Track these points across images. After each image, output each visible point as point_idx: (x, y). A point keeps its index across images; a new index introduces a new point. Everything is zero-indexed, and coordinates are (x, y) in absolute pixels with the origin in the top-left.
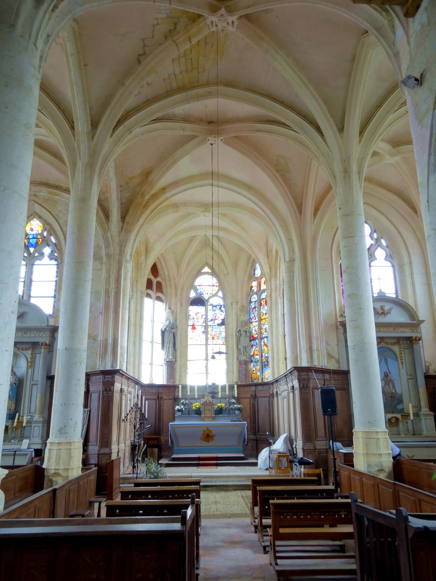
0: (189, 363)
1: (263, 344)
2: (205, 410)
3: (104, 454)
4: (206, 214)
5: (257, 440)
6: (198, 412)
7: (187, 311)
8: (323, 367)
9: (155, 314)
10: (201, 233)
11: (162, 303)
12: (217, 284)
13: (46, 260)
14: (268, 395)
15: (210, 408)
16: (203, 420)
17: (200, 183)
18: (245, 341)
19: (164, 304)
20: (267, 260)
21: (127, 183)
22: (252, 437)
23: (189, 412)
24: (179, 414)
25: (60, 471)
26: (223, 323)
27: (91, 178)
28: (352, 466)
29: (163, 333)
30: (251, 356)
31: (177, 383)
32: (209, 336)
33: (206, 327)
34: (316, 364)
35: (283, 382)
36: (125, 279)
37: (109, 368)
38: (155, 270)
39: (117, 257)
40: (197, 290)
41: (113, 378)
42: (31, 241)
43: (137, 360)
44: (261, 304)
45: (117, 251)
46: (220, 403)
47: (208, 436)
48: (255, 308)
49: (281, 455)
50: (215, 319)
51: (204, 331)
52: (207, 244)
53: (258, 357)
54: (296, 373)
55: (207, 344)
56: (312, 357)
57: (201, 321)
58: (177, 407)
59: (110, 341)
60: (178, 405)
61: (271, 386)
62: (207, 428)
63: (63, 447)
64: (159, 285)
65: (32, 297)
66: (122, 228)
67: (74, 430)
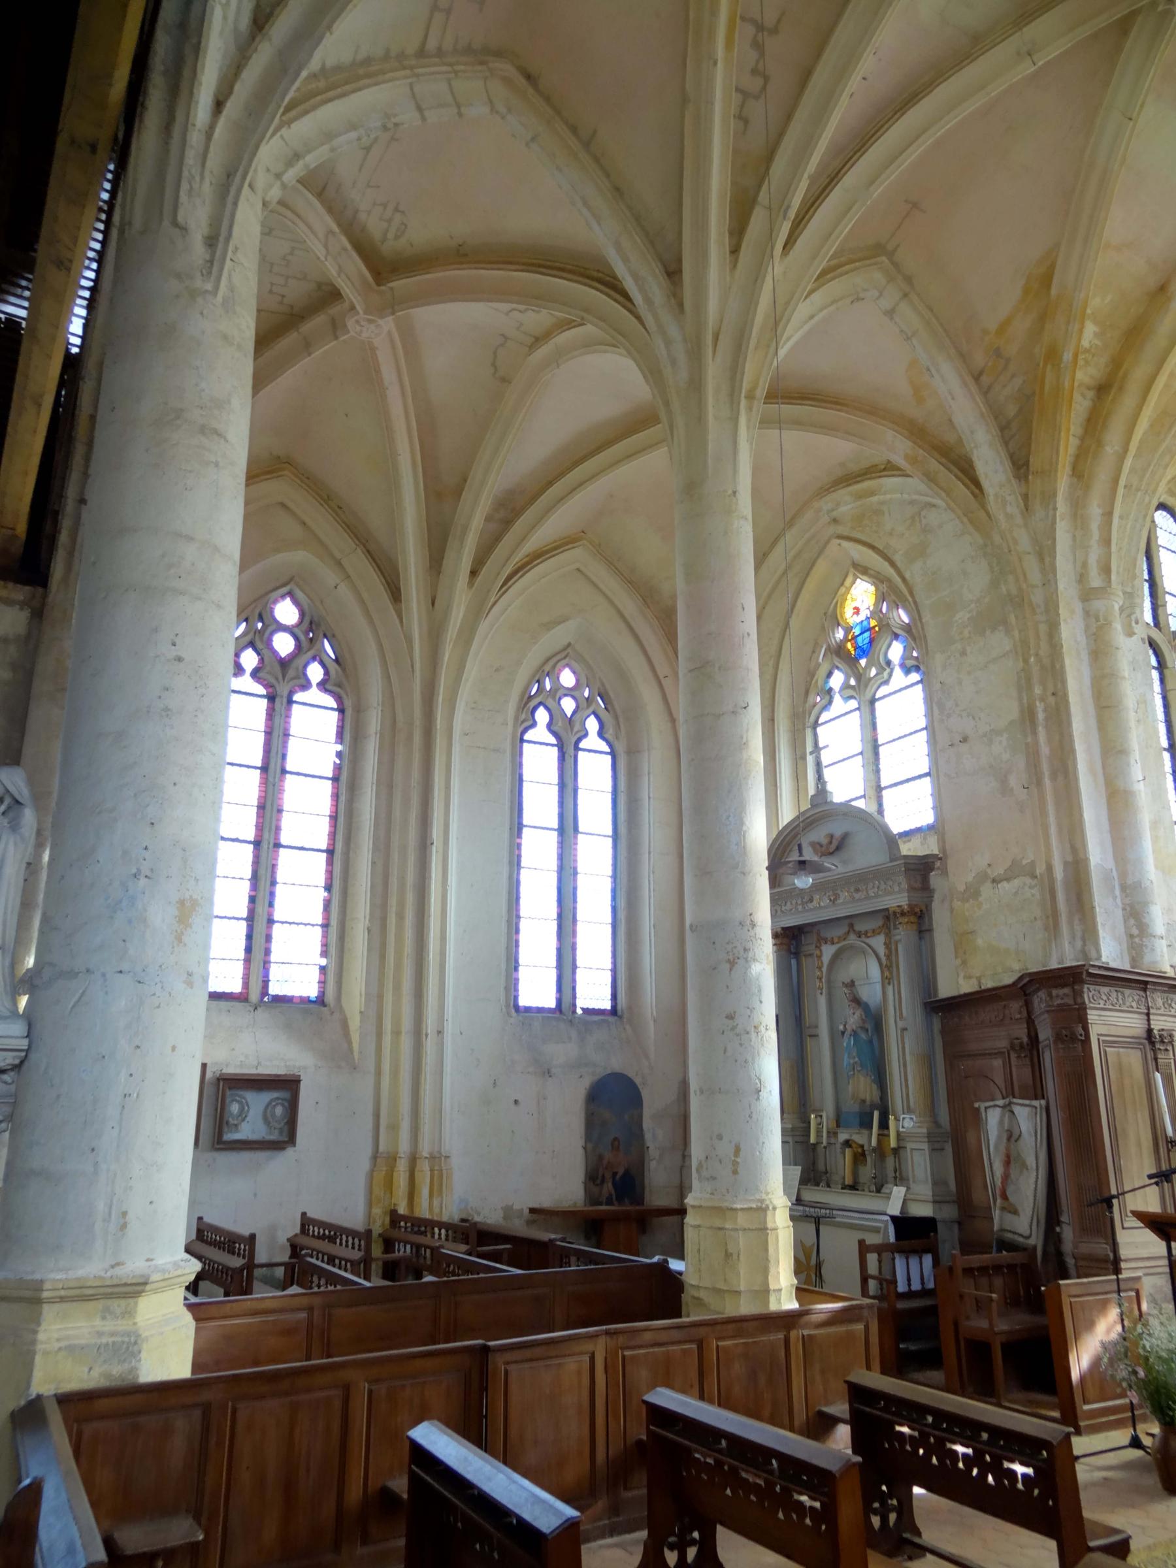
13: (899, 678)
21: (998, 353)
45: (1035, 576)
65: (886, 788)
66: (1025, 497)
67: (735, 1172)
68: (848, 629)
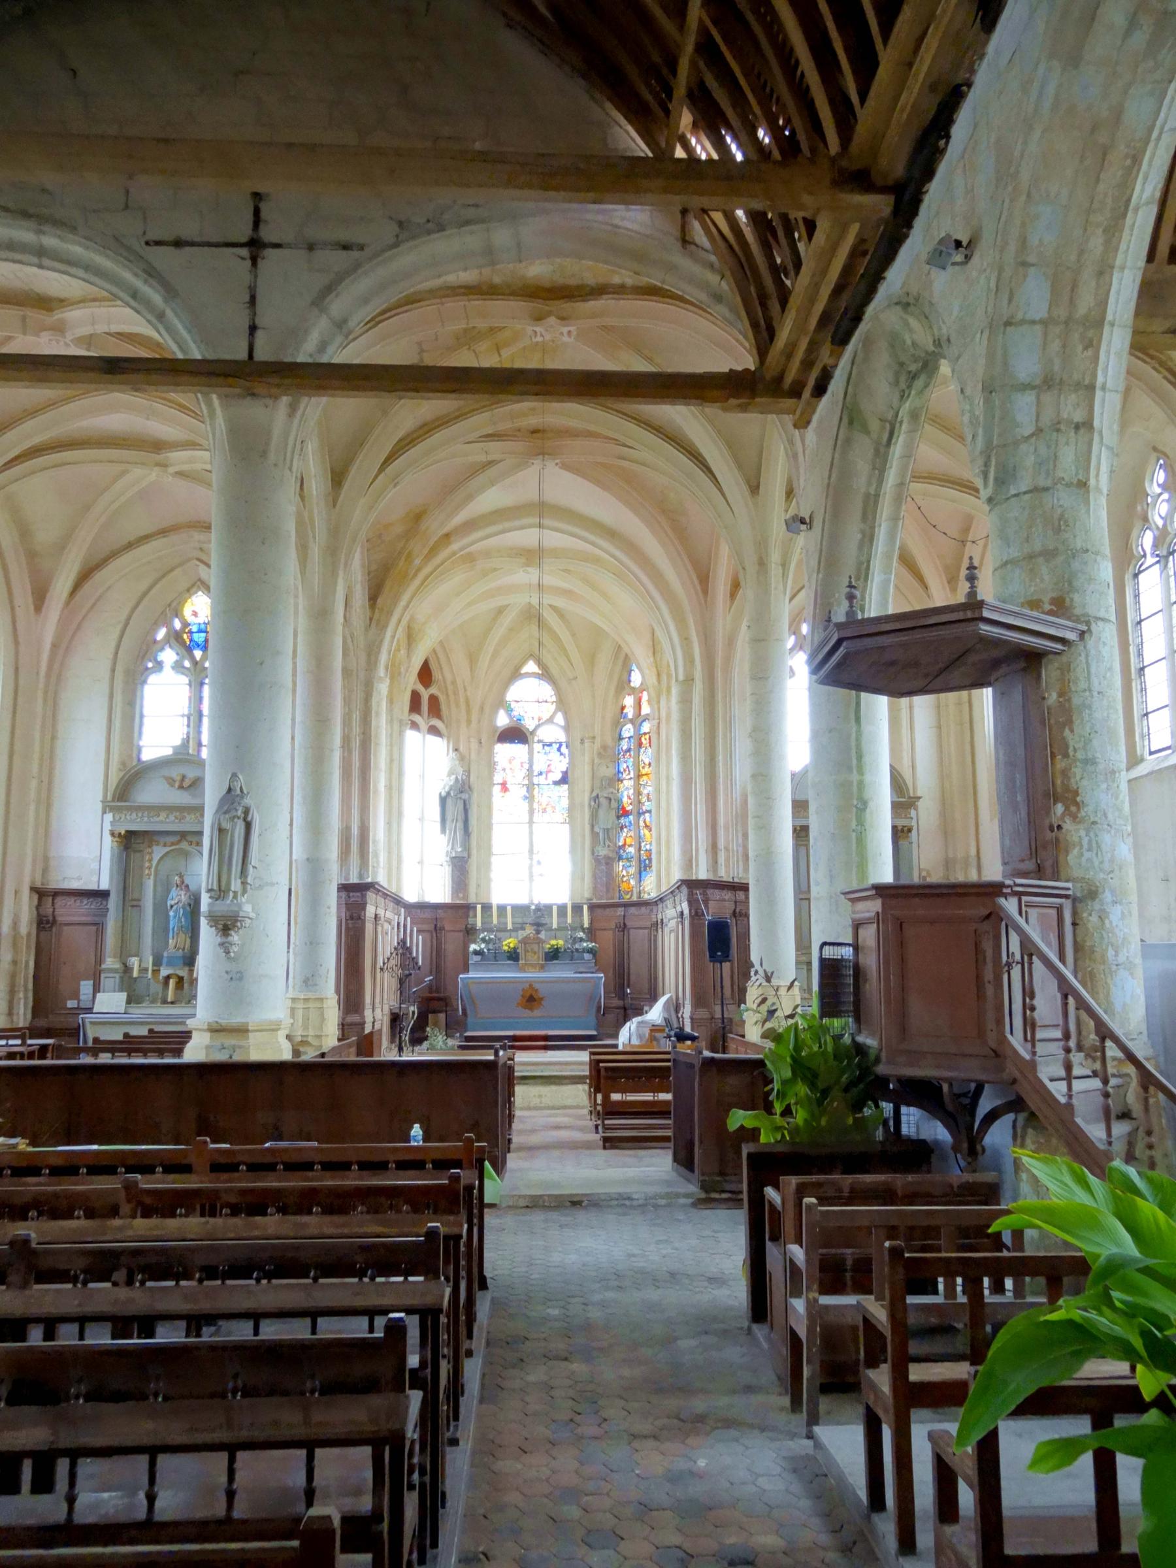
0: (493, 859)
1: (642, 824)
2: (526, 951)
3: (351, 1024)
4: (530, 569)
5: (625, 1009)
6: (513, 956)
7: (491, 753)
8: (736, 880)
9: (424, 762)
10: (520, 600)
11: (438, 739)
12: (554, 699)
14: (648, 924)
15: (535, 947)
16: (522, 970)
17: (517, 523)
18: (607, 818)
19: (445, 741)
20: (652, 659)
21: (380, 536)
22: (616, 1002)
23: (494, 956)
24: (478, 958)
25: (310, 1039)
26: (564, 780)
27: (334, 574)
28: (743, 1036)
29: (443, 801)
30: (620, 847)
31: (472, 899)
32: (535, 806)
33: (530, 787)
34: (724, 875)
35: (669, 903)
36: (378, 714)
37: (354, 879)
38: (425, 674)
39: (362, 675)
41: (364, 897)
42: (196, 637)
43: (395, 857)
44: (640, 745)
46: (555, 938)
47: (531, 1000)
48: (629, 750)
49: (655, 1029)
50: (548, 772)
52: (533, 616)
53: (631, 850)
54: (685, 890)
55: (531, 822)
56: (715, 862)
58: (473, 947)
59: (355, 831)
60: (475, 942)
61: (655, 908)
62: (531, 985)
63: (311, 1005)
64: (434, 700)
66: (371, 619)
68: (186, 624)
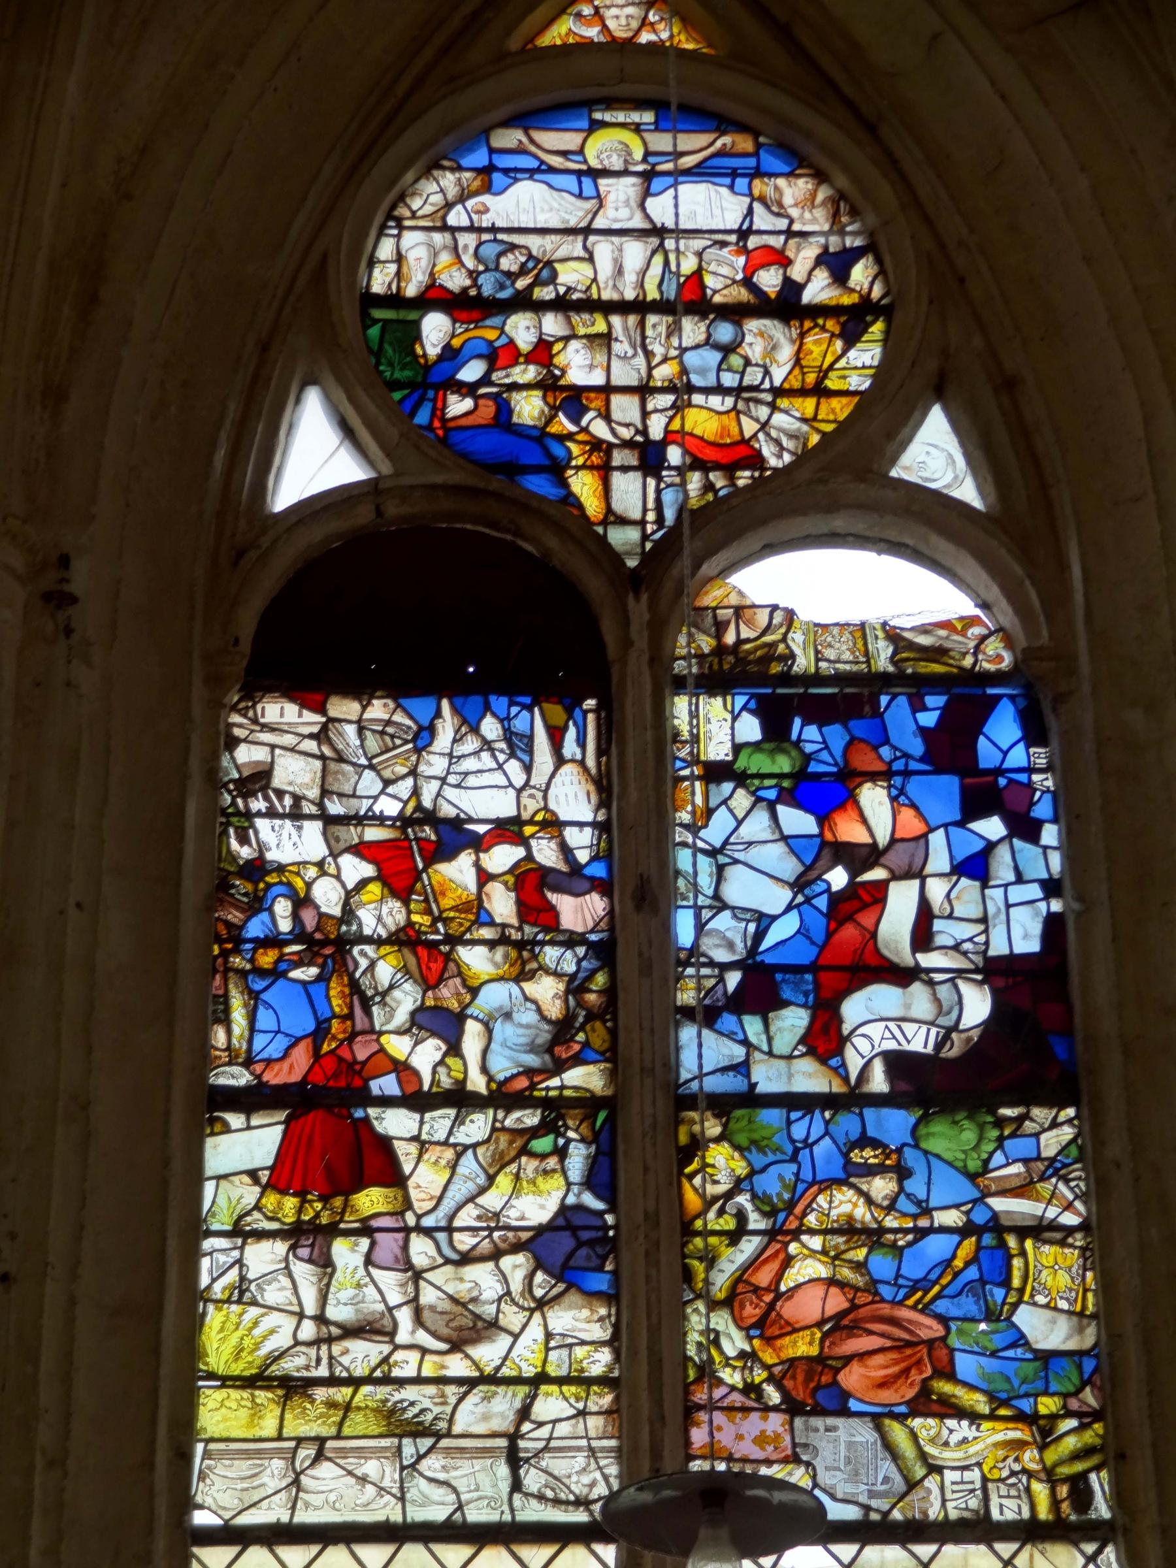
26: (1031, 1040)
40: (438, 378)
51: (567, 1218)
57: (512, 1013)
